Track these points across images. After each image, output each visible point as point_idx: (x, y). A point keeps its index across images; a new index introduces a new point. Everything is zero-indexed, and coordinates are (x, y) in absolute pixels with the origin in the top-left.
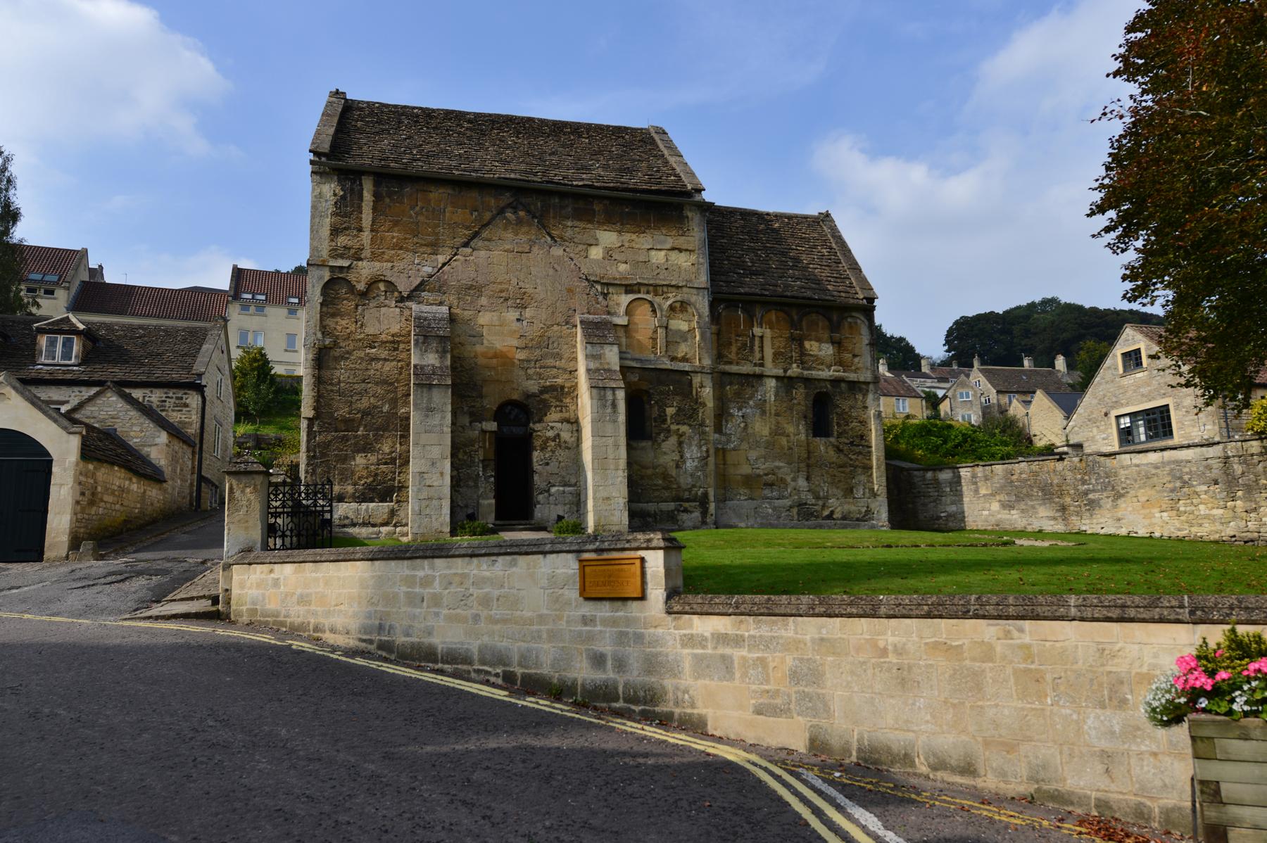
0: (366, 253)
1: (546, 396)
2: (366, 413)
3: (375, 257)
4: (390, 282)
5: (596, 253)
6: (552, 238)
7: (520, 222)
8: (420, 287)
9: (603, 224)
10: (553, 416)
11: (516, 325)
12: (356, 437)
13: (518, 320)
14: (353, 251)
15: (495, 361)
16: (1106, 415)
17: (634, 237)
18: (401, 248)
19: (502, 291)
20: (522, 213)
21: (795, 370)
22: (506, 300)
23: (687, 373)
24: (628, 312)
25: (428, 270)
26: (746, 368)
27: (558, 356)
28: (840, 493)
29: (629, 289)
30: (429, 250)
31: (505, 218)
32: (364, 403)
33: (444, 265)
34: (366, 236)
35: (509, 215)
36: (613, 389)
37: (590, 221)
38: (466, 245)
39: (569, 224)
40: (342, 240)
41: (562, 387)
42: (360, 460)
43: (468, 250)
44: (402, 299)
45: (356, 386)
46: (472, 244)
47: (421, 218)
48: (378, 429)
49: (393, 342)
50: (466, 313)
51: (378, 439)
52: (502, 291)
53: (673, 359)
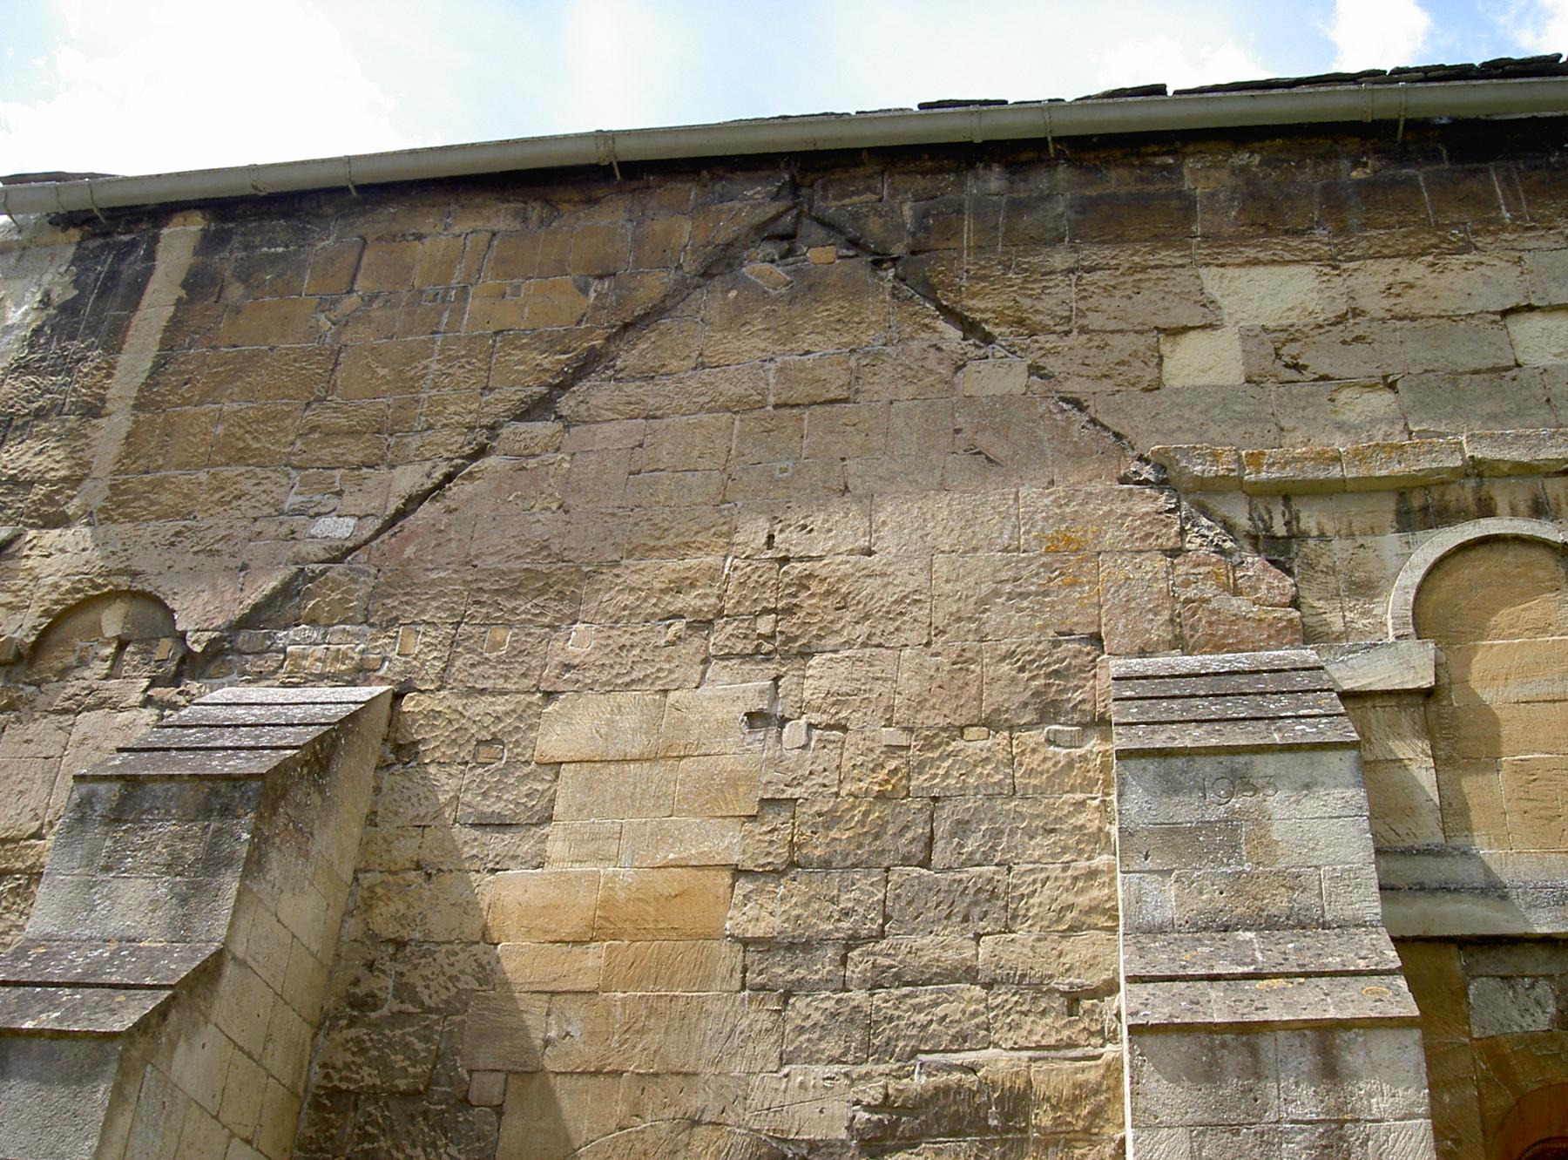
6: (970, 328)
7: (808, 288)
9: (1242, 239)
11: (740, 753)
13: (754, 719)
14: (40, 491)
15: (594, 956)
17: (1413, 270)
18: (240, 457)
19: (678, 587)
20: (820, 255)
22: (702, 624)
24: (1423, 622)
25: (339, 528)
27: (992, 906)
29: (1418, 505)
30: (356, 451)
31: (747, 284)
35: (761, 268)
36: (1326, 1041)
37: (1163, 240)
38: (531, 411)
39: (1060, 259)
41: (1017, 1101)
43: (542, 429)
46: (565, 404)
47: (359, 336)
50: (479, 707)
52: (678, 587)
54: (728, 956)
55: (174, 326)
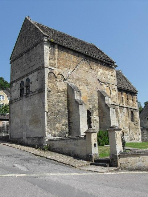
0: (56, 66)
1: (93, 109)
2: (59, 111)
3: (58, 68)
4: (62, 75)
5: (99, 74)
7: (86, 64)
8: (69, 77)
10: (95, 114)
12: (57, 118)
16: (145, 118)
19: (84, 81)
21: (128, 107)
23: (115, 105)
25: (69, 73)
26: (121, 105)
28: (135, 134)
32: (59, 108)
33: (72, 72)
34: (56, 61)
37: (98, 66)
38: (76, 67)
40: (52, 61)
42: (58, 125)
44: (65, 80)
45: (56, 103)
48: (62, 116)
49: (64, 92)
51: (62, 118)
52: (84, 81)
53: (114, 102)
54: (87, 100)
55: (58, 54)
